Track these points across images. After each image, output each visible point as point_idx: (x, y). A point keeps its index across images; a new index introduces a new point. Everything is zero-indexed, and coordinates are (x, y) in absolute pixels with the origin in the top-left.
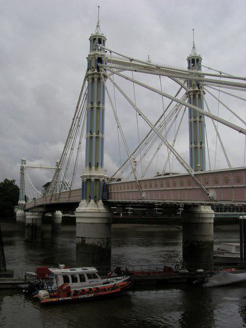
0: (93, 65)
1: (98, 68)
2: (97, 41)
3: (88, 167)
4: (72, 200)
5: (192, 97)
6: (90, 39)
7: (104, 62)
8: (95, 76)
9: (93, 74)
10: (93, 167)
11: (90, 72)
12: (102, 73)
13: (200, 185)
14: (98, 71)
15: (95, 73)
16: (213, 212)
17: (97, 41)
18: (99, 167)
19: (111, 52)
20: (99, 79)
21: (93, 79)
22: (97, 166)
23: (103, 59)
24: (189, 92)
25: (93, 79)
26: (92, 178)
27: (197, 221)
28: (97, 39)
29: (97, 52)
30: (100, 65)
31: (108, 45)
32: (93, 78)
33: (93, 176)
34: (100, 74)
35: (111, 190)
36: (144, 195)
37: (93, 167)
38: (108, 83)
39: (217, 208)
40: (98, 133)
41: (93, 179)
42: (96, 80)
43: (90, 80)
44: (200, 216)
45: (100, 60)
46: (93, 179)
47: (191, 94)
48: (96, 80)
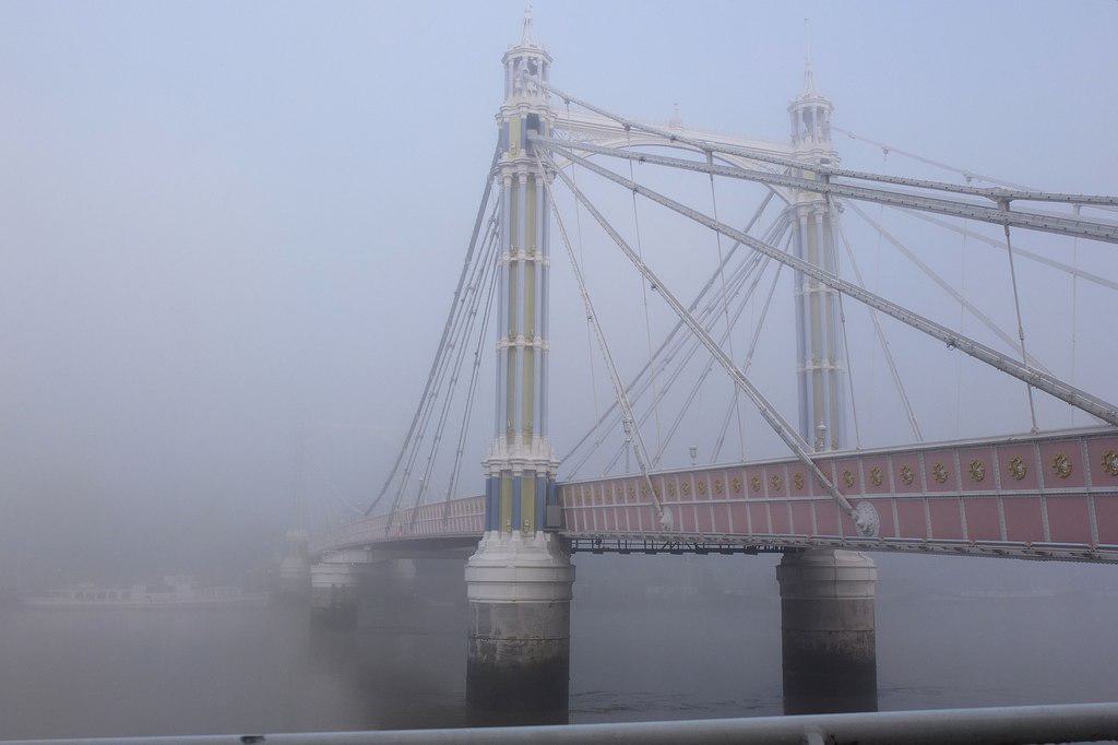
0: (515, 137)
2: (526, 67)
3: (503, 437)
4: (459, 527)
5: (804, 221)
7: (547, 132)
9: (514, 165)
10: (519, 437)
11: (506, 158)
13: (829, 491)
17: (526, 67)
18: (536, 436)
19: (567, 102)
20: (532, 178)
21: (515, 178)
22: (529, 432)
23: (542, 119)
24: (797, 207)
25: (515, 178)
28: (525, 60)
29: (525, 98)
30: (533, 135)
31: (557, 77)
32: (514, 174)
33: (522, 462)
35: (570, 503)
38: (558, 189)
42: (523, 180)
43: (508, 182)
45: (533, 122)
47: (803, 212)
48: (523, 180)
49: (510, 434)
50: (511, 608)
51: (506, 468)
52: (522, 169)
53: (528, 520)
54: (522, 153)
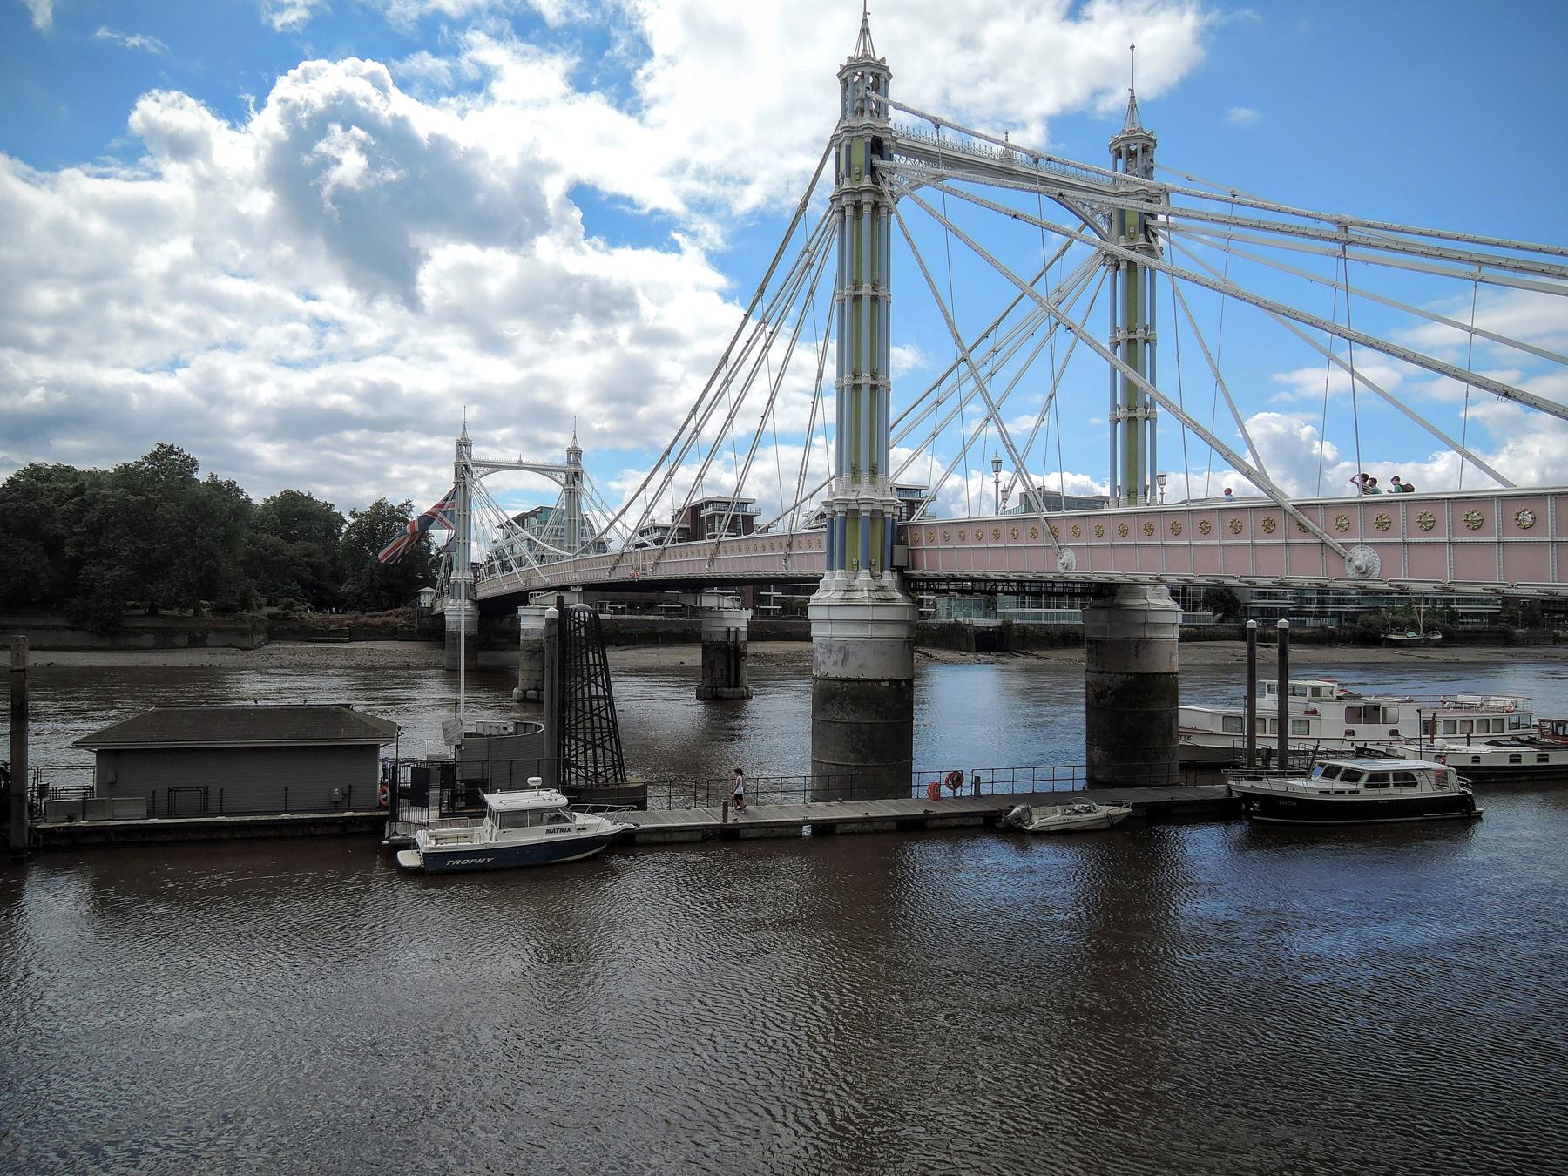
1: (873, 170)
3: (847, 476)
6: (840, 75)
8: (866, 198)
10: (865, 476)
11: (846, 185)
12: (886, 188)
14: (876, 182)
15: (870, 191)
16: (1178, 607)
19: (937, 126)
20: (876, 207)
21: (858, 207)
23: (886, 143)
25: (858, 207)
26: (862, 508)
27: (1138, 634)
29: (866, 120)
30: (878, 162)
33: (868, 502)
34: (881, 194)
36: (1068, 556)
37: (865, 476)
39: (1181, 594)
40: (874, 375)
41: (865, 509)
42: (867, 209)
44: (1143, 619)
45: (877, 147)
46: (865, 509)
48: (867, 209)
49: (855, 471)
50: (865, 643)
51: (856, 507)
52: (866, 198)
53: (876, 561)
54: (867, 182)
